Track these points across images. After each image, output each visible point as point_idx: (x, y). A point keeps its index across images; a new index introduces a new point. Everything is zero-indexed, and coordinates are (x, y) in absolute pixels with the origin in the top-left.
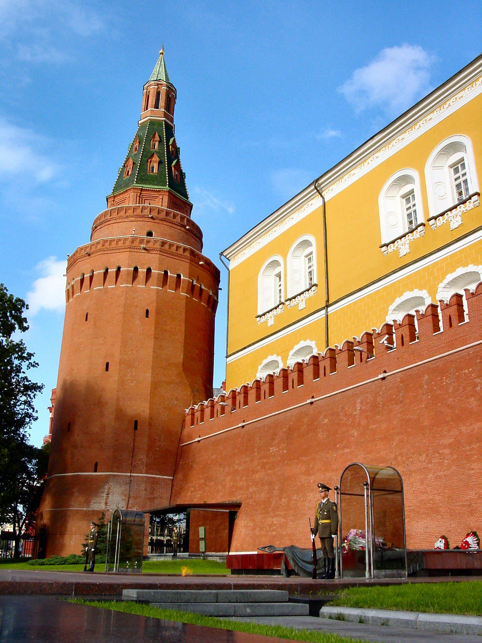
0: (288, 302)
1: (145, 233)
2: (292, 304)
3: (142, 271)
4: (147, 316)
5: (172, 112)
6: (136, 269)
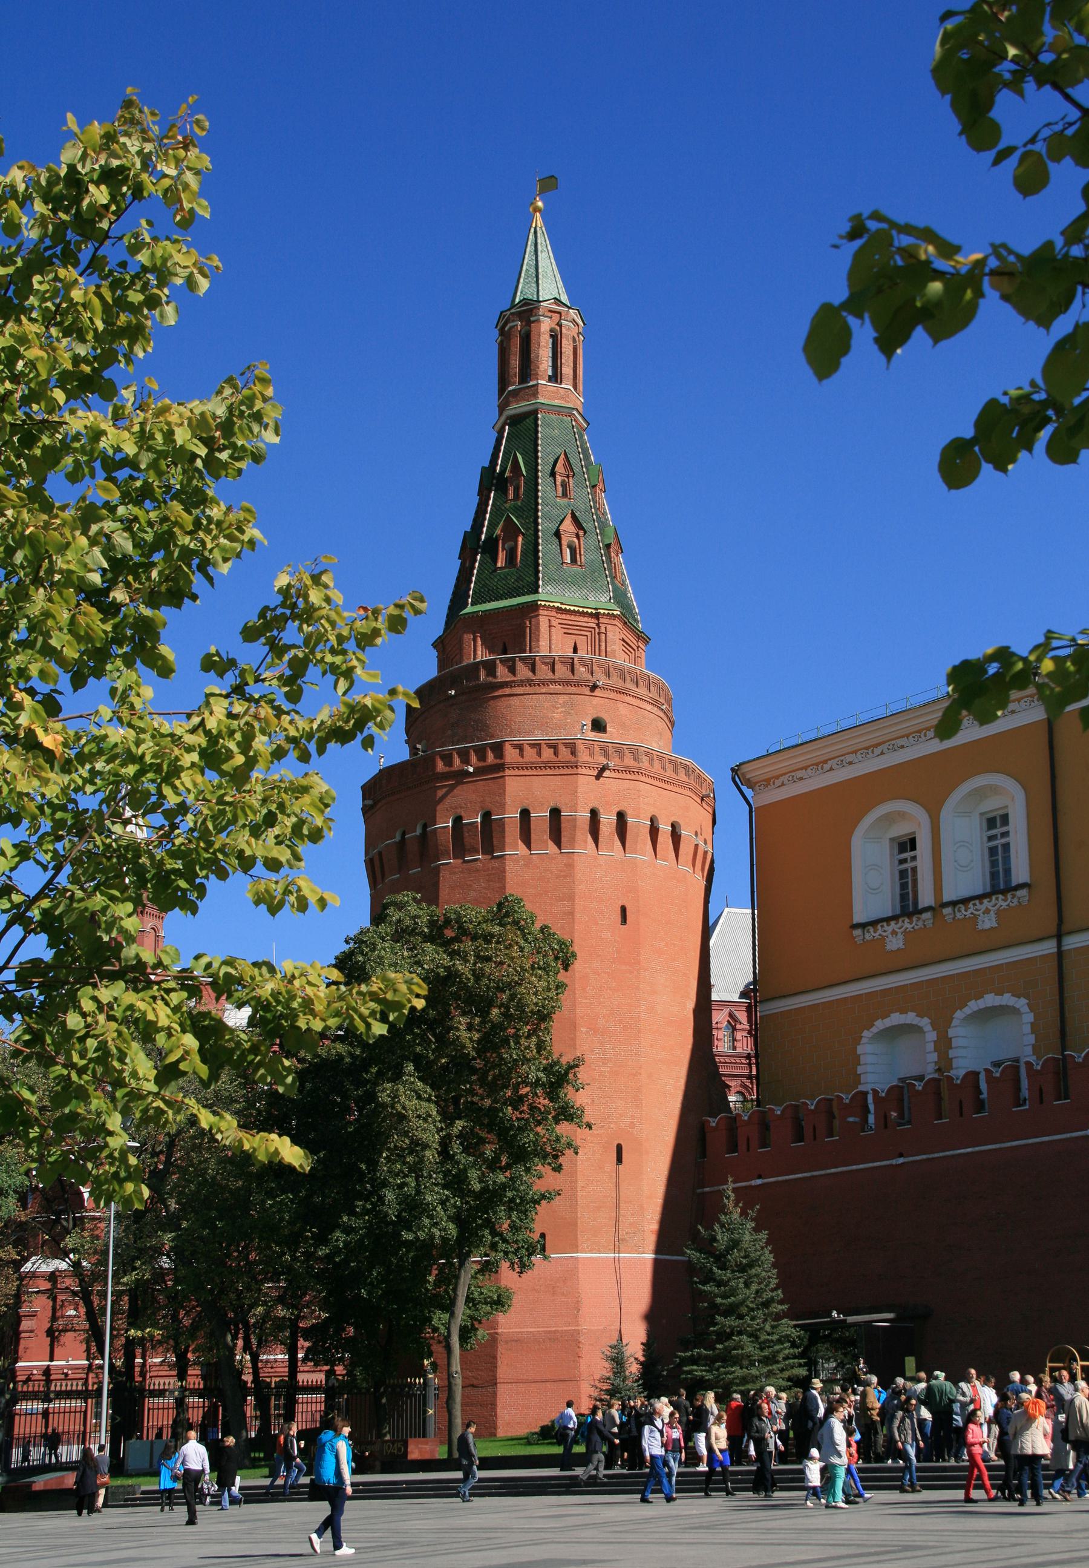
0: (947, 911)
4: (624, 920)
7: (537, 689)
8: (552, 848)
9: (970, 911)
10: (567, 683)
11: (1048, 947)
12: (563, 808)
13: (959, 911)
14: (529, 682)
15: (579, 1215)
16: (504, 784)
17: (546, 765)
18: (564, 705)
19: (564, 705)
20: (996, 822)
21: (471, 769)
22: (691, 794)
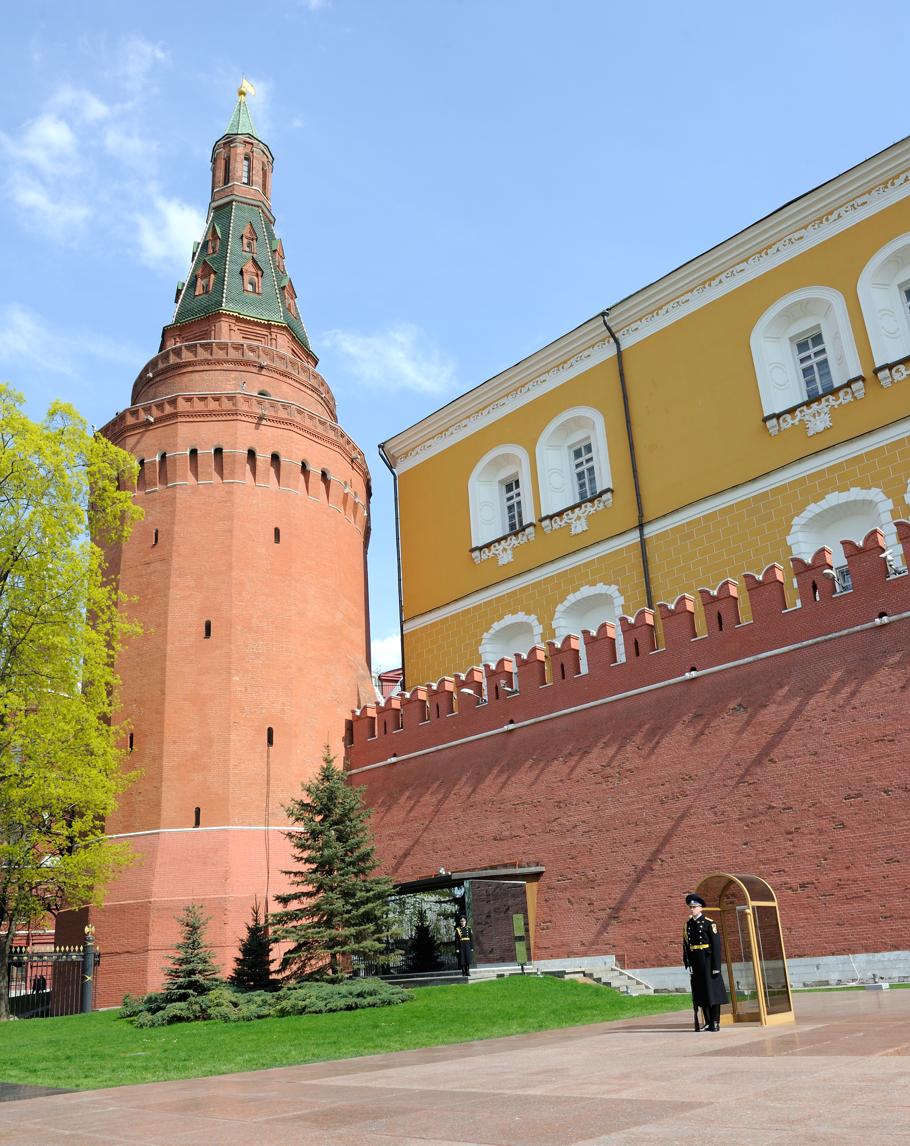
0: (547, 522)
2: (555, 526)
7: (213, 367)
8: (216, 478)
9: (564, 521)
10: (237, 362)
11: (634, 537)
12: (223, 448)
13: (555, 522)
14: (207, 362)
15: (231, 790)
16: (177, 428)
17: (211, 413)
18: (234, 379)
19: (234, 379)
20: (582, 452)
21: (152, 420)
22: (340, 452)
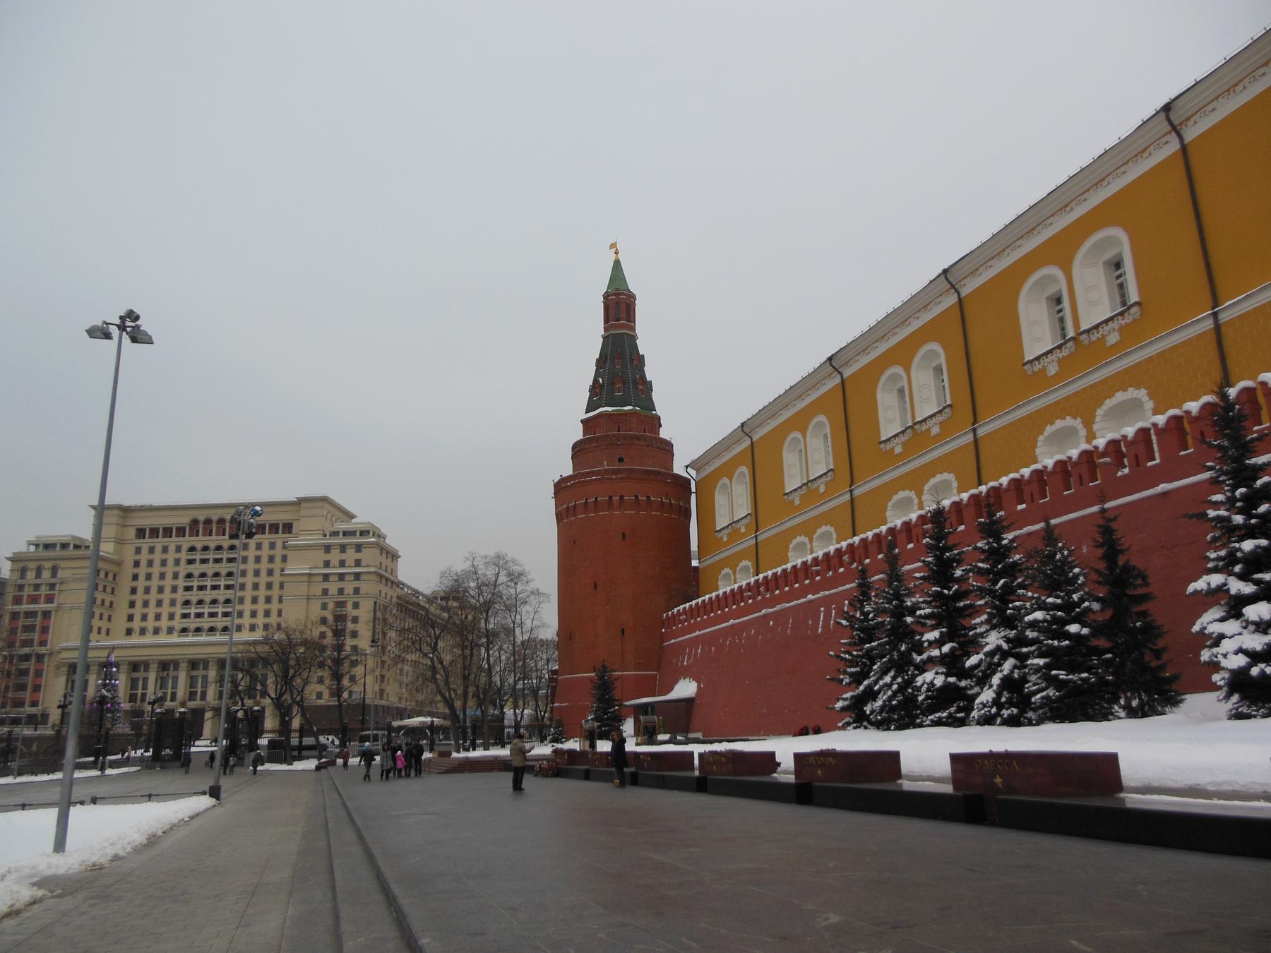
1: (617, 459)
3: (616, 498)
4: (624, 538)
5: (633, 320)
6: (611, 497)
